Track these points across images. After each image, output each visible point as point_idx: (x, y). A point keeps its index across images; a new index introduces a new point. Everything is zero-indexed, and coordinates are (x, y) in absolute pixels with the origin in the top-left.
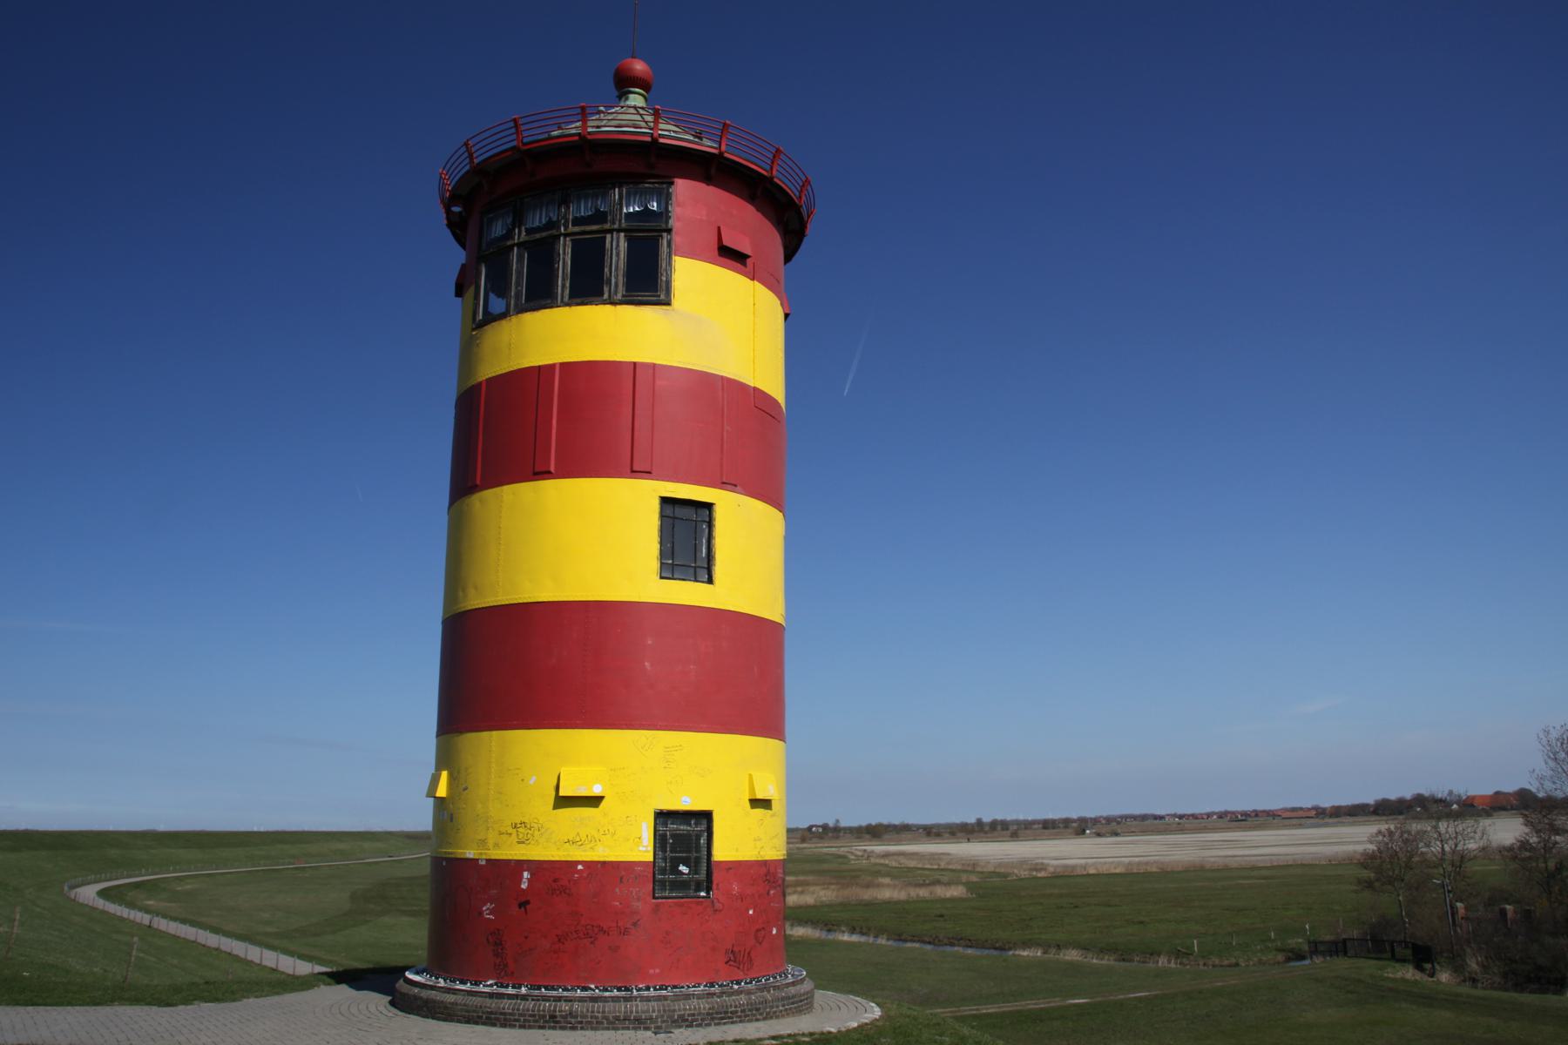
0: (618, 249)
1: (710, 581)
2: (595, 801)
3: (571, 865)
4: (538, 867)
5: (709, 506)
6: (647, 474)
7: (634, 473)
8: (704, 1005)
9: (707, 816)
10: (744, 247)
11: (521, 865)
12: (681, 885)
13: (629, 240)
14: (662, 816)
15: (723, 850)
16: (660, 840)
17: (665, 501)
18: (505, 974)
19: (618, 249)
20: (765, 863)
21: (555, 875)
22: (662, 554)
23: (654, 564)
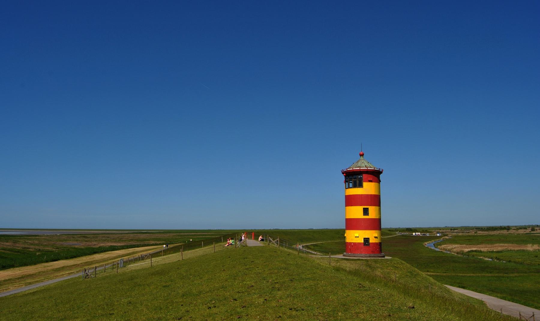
0: (358, 182)
1: (369, 215)
2: (358, 237)
3: (356, 243)
4: (353, 243)
5: (368, 208)
6: (362, 206)
7: (360, 206)
8: (368, 256)
9: (369, 238)
10: (371, 180)
11: (352, 243)
12: (367, 245)
13: (359, 181)
14: (364, 238)
15: (371, 241)
16: (364, 241)
17: (364, 208)
18: (351, 252)
19: (358, 182)
20: (376, 243)
21: (355, 244)
22: (363, 213)
23: (363, 214)
